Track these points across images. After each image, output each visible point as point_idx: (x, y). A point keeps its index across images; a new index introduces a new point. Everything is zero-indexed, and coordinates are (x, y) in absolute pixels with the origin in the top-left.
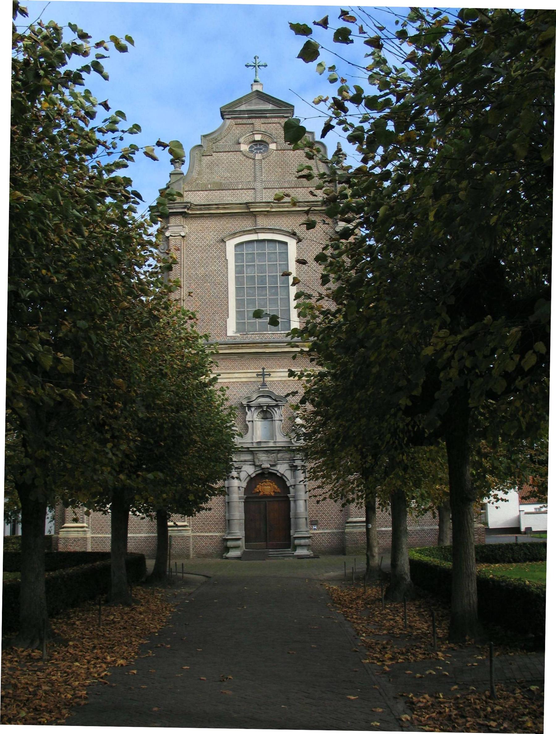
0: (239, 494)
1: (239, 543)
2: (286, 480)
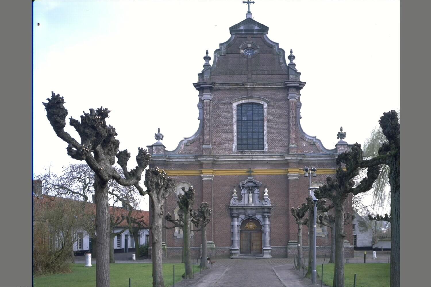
0: (238, 228)
1: (238, 251)
2: (260, 222)
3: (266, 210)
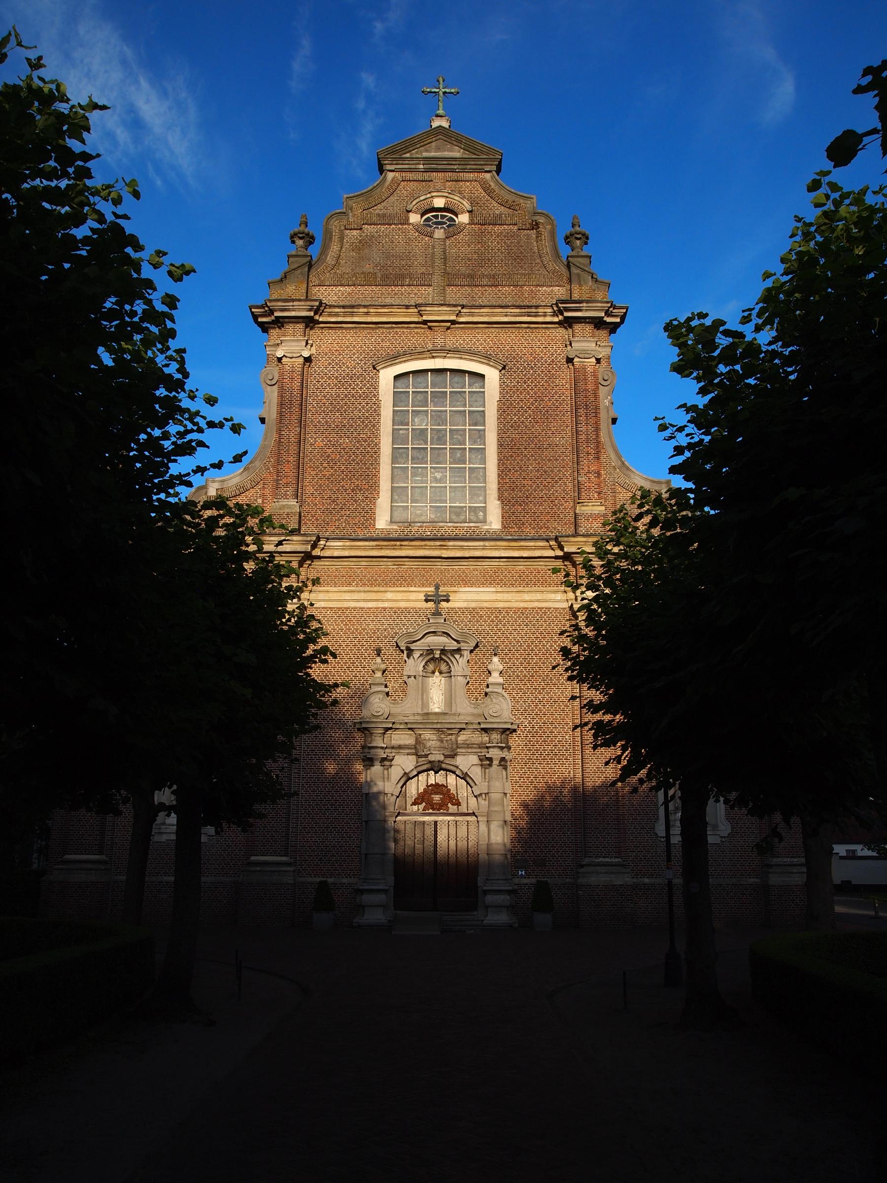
3: (495, 736)
